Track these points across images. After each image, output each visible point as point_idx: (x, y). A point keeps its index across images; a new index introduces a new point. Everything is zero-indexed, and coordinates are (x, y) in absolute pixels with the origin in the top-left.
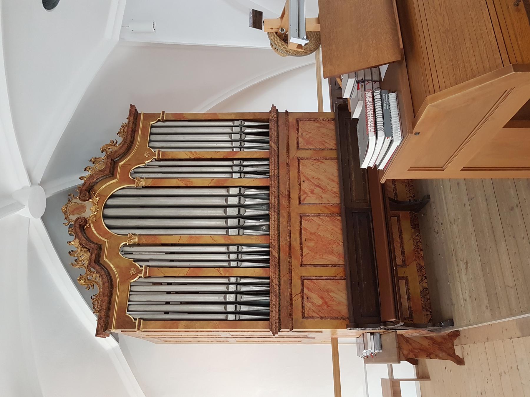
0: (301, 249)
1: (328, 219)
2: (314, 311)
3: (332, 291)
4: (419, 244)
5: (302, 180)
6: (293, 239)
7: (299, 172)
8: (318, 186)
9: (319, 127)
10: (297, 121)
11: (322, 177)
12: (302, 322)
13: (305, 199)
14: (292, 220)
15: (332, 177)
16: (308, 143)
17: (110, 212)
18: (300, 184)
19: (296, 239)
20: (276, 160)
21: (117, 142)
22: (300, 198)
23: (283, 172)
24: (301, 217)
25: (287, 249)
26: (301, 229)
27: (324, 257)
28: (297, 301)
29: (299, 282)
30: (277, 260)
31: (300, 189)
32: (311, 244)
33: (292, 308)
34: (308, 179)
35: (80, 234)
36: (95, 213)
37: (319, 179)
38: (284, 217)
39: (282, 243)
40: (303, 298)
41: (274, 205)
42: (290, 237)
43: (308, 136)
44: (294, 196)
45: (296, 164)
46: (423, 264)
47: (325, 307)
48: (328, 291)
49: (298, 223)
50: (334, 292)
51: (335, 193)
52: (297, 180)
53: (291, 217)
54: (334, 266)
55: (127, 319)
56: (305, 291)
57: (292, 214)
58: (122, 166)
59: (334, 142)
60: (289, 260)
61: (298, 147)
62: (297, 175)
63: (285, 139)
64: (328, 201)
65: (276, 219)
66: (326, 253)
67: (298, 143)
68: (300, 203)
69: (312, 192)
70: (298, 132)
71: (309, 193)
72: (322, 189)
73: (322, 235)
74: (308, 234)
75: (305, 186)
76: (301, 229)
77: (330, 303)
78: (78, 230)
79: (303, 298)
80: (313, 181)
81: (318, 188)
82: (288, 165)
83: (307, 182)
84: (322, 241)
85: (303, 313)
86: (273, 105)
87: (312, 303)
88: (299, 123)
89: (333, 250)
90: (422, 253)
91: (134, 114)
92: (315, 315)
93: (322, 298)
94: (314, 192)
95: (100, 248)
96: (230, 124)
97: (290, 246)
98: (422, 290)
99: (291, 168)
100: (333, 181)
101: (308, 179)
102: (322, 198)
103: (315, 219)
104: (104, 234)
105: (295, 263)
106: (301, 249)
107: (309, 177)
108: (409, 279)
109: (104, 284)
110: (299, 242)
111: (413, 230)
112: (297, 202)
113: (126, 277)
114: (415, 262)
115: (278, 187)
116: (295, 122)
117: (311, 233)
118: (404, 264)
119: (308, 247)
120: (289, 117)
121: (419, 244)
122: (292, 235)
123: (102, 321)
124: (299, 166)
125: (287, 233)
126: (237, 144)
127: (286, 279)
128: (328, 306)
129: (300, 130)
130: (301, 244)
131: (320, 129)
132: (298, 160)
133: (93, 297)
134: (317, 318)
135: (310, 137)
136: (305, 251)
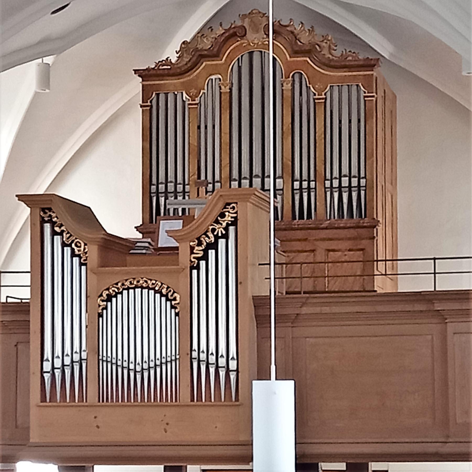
5: (289, 254)
7: (299, 252)
10: (362, 250)
15: (294, 286)
21: (335, 50)
45: (308, 249)
61: (329, 251)
62: (295, 249)
67: (333, 251)
70: (350, 250)
78: (231, 31)
95: (216, 55)
99: (304, 243)
109: (178, 68)
113: (187, 87)
120: (368, 241)
124: (306, 251)
126: (336, 183)
132: (313, 251)
133: (169, 59)
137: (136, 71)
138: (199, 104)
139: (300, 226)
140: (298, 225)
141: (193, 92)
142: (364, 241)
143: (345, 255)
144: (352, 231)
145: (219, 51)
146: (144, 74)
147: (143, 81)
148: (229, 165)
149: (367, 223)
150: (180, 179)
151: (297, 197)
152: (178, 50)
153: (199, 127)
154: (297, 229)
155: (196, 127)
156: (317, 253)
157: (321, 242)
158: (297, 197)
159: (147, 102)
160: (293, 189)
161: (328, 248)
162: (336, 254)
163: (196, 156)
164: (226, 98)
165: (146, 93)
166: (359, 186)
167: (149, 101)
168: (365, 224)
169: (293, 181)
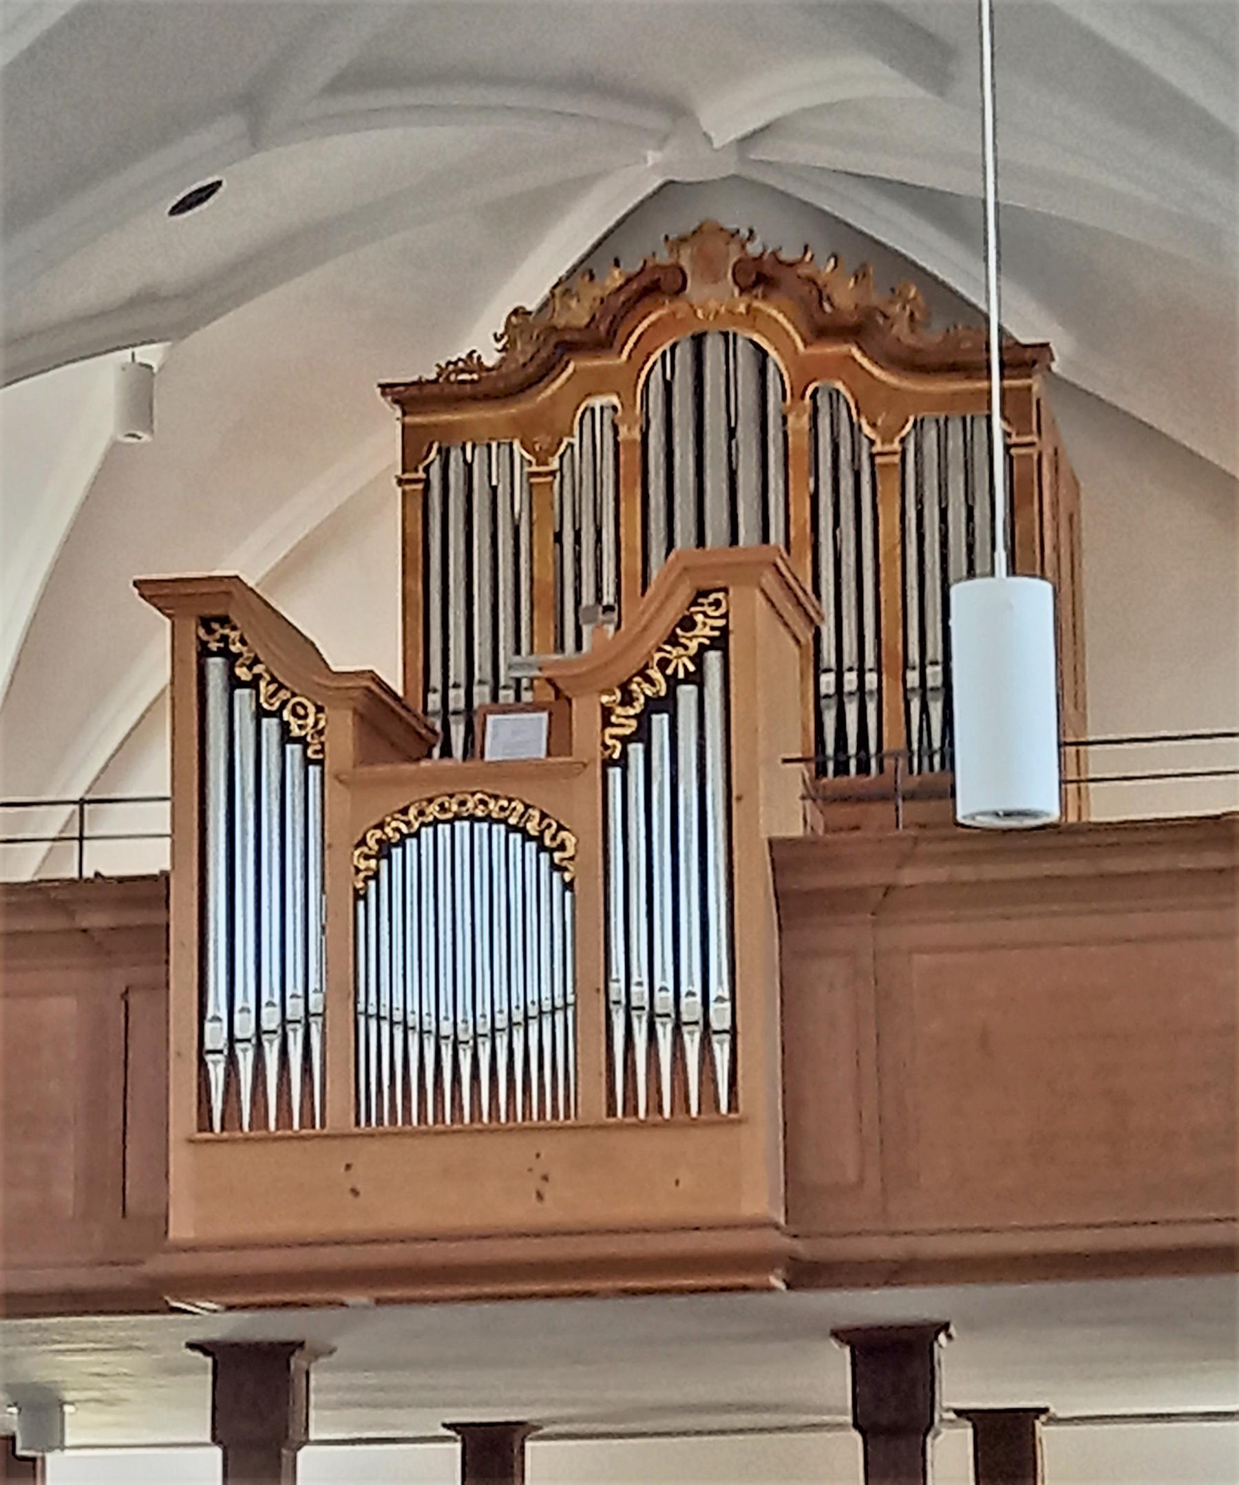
17: (713, 349)
35: (634, 286)
95: (605, 343)
113: (525, 431)
133: (475, 355)
138: (558, 475)
141: (542, 441)
145: (612, 332)
146: (407, 397)
147: (404, 414)
152: (501, 330)
153: (558, 537)
155: (551, 538)
159: (416, 470)
163: (552, 613)
164: (630, 458)
165: (414, 447)
167: (421, 468)
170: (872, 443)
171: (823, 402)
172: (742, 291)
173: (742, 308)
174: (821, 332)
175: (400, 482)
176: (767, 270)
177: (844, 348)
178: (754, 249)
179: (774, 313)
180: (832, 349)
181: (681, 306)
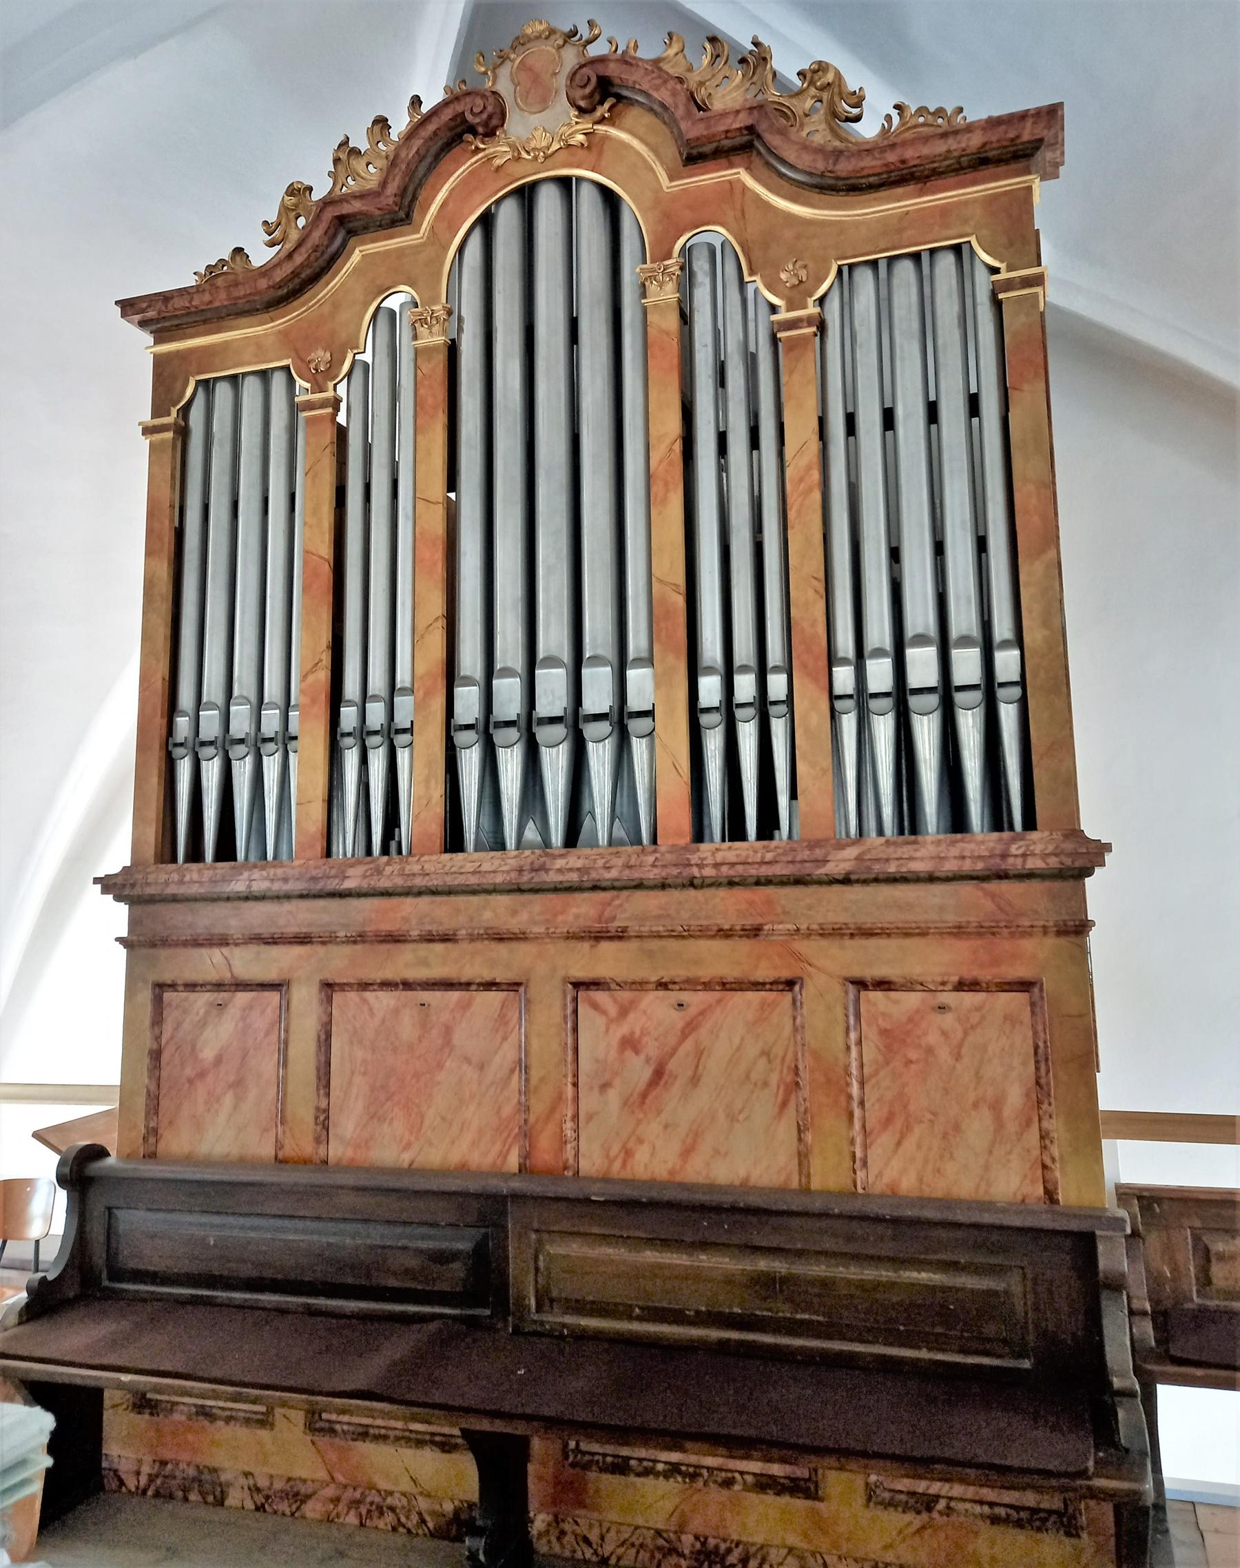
0: (386, 985)
1: (508, 1110)
2: (178, 1026)
3: (239, 1099)
4: (389, 1518)
5: (685, 996)
6: (424, 949)
7: (725, 986)
8: (659, 1074)
9: (996, 1106)
10: (1024, 986)
11: (702, 1098)
12: (145, 981)
13: (595, 1006)
14: (502, 950)
16: (893, 1039)
18: (663, 985)
19: (424, 963)
20: (765, 871)
22: (595, 984)
23: (726, 906)
24: (514, 986)
25: (386, 927)
26: (466, 986)
27: (358, 1079)
28: (210, 964)
29: (272, 975)
30: (333, 885)
31: (639, 986)
32: (407, 1027)
33: (185, 944)
34: (690, 1028)
36: (524, 155)
37: (695, 1080)
38: (514, 913)
39: (408, 905)
40: (219, 986)
41: (543, 868)
42: (430, 938)
43: (933, 1038)
44: (607, 961)
45: (764, 973)
46: (313, 1509)
47: (189, 1072)
48: (238, 1084)
49: (487, 975)
50: (236, 1107)
51: (628, 1154)
52: (679, 973)
53: (514, 945)
54: (324, 1121)
55: (179, 385)
56: (243, 997)
57: (522, 947)
58: (733, 188)
59: (908, 1185)
60: (341, 934)
62: (705, 973)
63: (909, 917)
64: (590, 1117)
65: (489, 880)
66: (373, 1089)
67: (883, 985)
68: (577, 985)
69: (630, 1044)
70: (961, 986)
71: (623, 1030)
72: (644, 1096)
73: (441, 1077)
74: (445, 1017)
75: (657, 1011)
76: (466, 986)
77: (201, 1091)
79: (219, 986)
80: (681, 1051)
81: (647, 1073)
82: (755, 932)
83: (677, 1019)
84: (417, 1076)
85: (173, 986)
86: (1108, 847)
87: (203, 1024)
88: (1020, 998)
89: (382, 1119)
90: (352, 1519)
91: (1022, 144)
92: (168, 1029)
93: (218, 1060)
94: (629, 1054)
96: (1002, 628)
97: (394, 939)
98: (224, 1477)
100: (687, 1152)
101: (690, 1028)
102: (605, 1086)
103: (508, 1054)
104: (449, 219)
105: (339, 961)
106: (386, 985)
107: (703, 1032)
108: (264, 1434)
110: (413, 974)
111: (448, 1507)
112: (580, 974)
114: (322, 1474)
115: (639, 886)
116: (1020, 971)
117: (448, 1031)
118: (315, 1425)
119: (396, 1012)
120: (1051, 941)
121: (389, 1518)
122: (439, 947)
123: (160, 305)
124: (757, 986)
125: (447, 926)
127: (282, 922)
128: (191, 1081)
129: (969, 998)
130: (407, 985)
131: (985, 1112)
132: (790, 984)
134: (158, 1038)
135: (930, 1050)
136: (383, 1001)
137: (128, 307)
139: (724, 870)
140: (717, 865)
142: (1028, 945)
143: (942, 1008)
144: (967, 890)
146: (158, 314)
147: (158, 342)
148: (442, 623)
149: (1044, 856)
150: (273, 688)
151: (714, 744)
152: (272, 218)
154: (715, 884)
156: (808, 993)
157: (824, 943)
158: (714, 744)
160: (694, 709)
161: (857, 972)
162: (897, 1002)
166: (989, 686)
168: (1033, 864)
169: (694, 671)
170: (773, 309)
171: (701, 266)
172: (582, 111)
173: (580, 138)
174: (695, 157)
175: (147, 431)
176: (612, 70)
177: (727, 174)
178: (594, 50)
179: (623, 136)
180: (709, 178)
181: (499, 150)
